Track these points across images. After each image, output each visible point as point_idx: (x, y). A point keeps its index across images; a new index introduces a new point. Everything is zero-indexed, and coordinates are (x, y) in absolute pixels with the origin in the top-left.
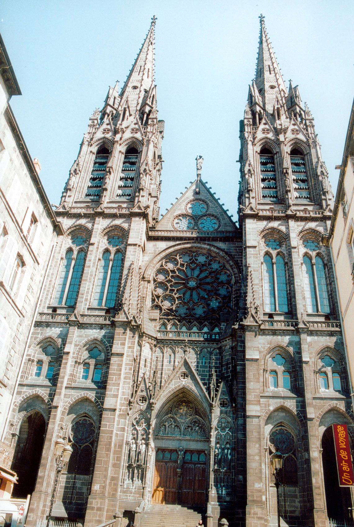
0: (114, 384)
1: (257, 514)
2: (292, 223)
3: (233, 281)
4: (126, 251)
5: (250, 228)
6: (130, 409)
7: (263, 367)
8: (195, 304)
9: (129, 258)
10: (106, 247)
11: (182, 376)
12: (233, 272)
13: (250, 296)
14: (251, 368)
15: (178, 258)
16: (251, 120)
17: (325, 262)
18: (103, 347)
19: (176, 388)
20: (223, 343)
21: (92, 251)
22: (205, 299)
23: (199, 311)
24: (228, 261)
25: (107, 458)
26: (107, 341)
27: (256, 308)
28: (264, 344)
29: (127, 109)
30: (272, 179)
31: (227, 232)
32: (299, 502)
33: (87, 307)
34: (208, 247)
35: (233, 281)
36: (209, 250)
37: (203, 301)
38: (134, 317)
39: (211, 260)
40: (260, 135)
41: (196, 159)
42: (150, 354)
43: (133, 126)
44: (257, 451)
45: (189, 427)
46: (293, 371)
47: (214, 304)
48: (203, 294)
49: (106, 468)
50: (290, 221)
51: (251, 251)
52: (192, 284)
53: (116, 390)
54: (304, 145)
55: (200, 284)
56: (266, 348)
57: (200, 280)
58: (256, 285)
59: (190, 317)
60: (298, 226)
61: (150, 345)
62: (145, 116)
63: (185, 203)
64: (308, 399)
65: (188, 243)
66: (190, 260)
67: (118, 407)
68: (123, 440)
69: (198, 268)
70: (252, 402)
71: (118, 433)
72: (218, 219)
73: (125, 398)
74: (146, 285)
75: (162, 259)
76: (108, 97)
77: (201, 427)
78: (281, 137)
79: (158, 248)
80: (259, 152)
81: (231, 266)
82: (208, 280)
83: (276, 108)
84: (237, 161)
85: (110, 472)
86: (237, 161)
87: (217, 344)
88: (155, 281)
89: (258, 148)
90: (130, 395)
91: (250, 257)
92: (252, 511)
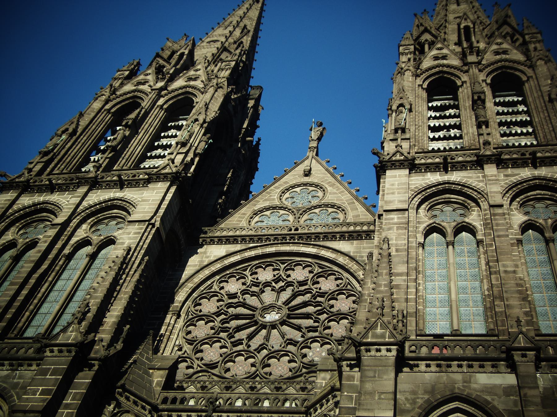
2: (491, 170)
9: (123, 243)
10: (85, 235)
15: (247, 273)
28: (414, 392)
37: (290, 348)
50: (485, 166)
51: (393, 219)
52: (272, 317)
54: (522, 67)
55: (289, 317)
56: (420, 401)
57: (291, 309)
58: (400, 274)
63: (278, 191)
72: (343, 210)
79: (207, 257)
91: (389, 229)
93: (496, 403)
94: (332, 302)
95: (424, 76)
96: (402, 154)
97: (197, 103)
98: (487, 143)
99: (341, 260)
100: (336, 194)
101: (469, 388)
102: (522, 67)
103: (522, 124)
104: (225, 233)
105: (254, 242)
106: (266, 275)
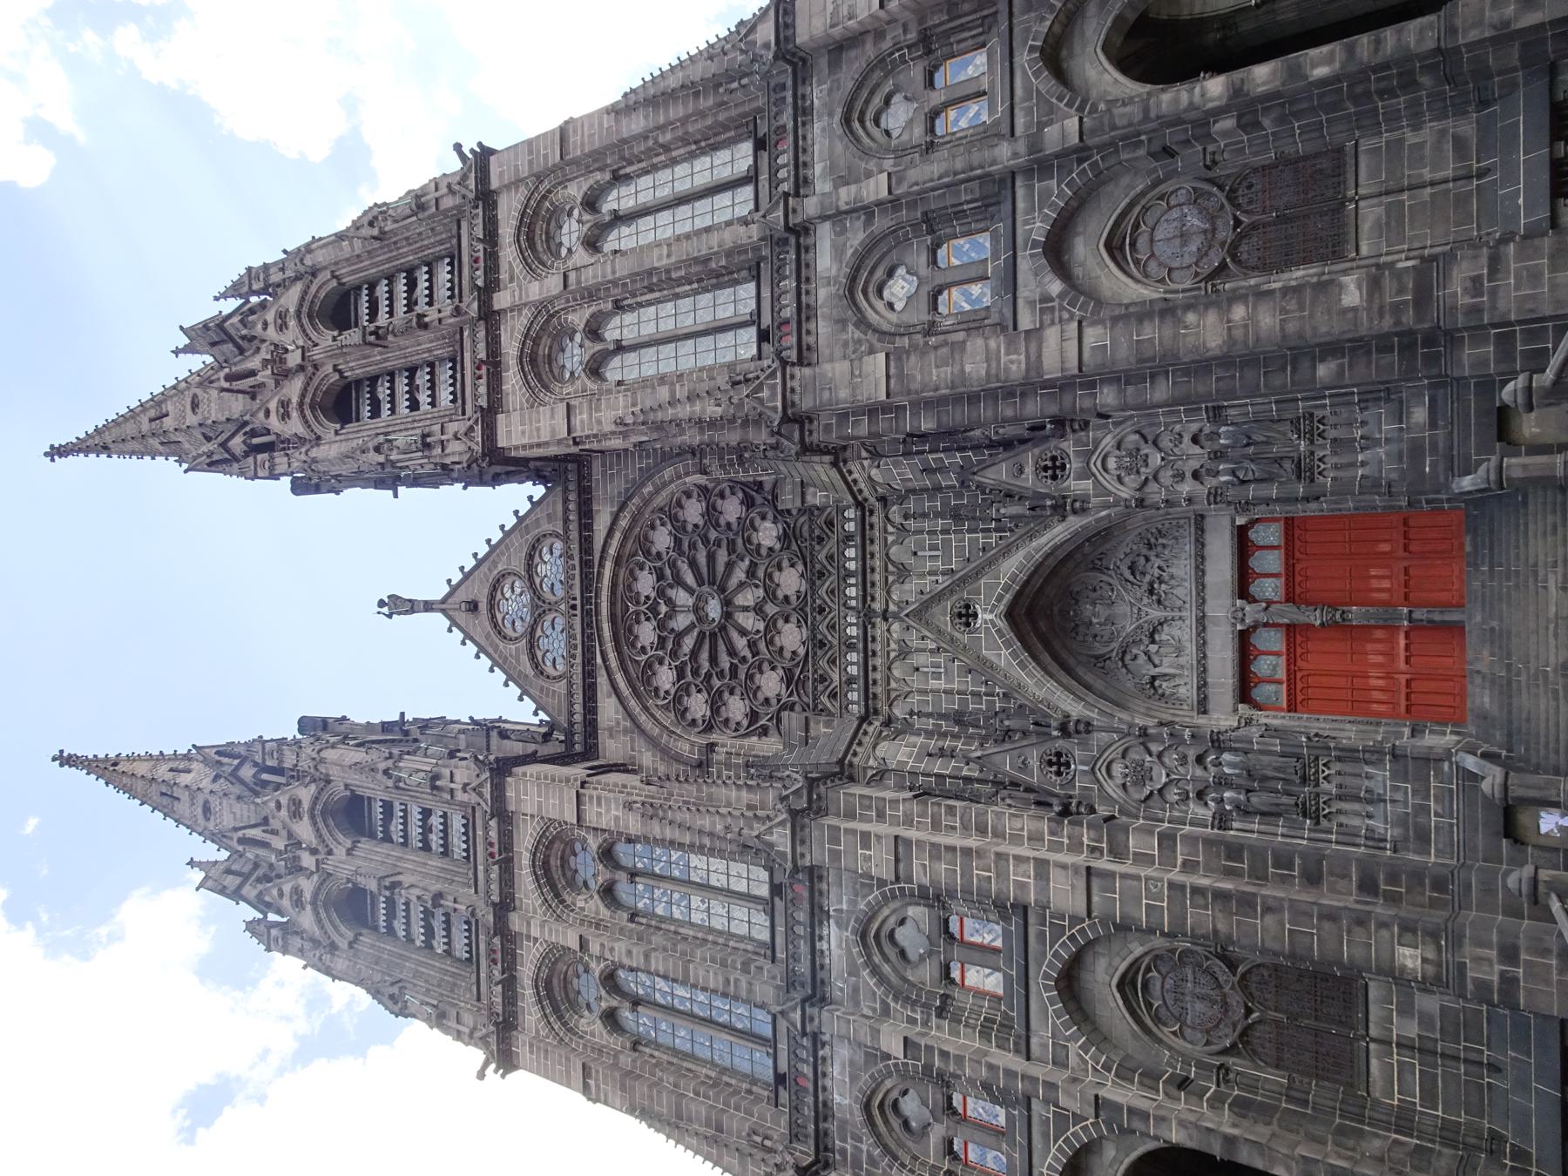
0: (1002, 875)
1: (1476, 280)
2: (501, 300)
3: (700, 479)
4: (604, 831)
5: (523, 433)
6: (1092, 810)
7: (919, 338)
8: (771, 594)
9: (617, 818)
10: (596, 897)
11: (968, 624)
12: (672, 481)
13: (703, 410)
14: (919, 377)
15: (644, 657)
16: (260, 457)
17: (608, 176)
18: (886, 912)
19: (1008, 644)
20: (866, 493)
21: (602, 945)
22: (753, 565)
23: (790, 581)
24: (647, 502)
25: (1280, 910)
26: (865, 897)
27: (735, 384)
28: (846, 344)
29: (240, 834)
30: (411, 378)
31: (566, 510)
32: (1416, 127)
33: (767, 965)
34: (609, 565)
35: (700, 479)
36: (617, 562)
37: (761, 573)
38: (783, 799)
39: (647, 553)
40: (295, 426)
41: (390, 616)
42: (913, 739)
43: (284, 813)
44: (1212, 317)
45: (1151, 591)
46: (931, 231)
47: (768, 534)
48: (739, 574)
49: (1321, 917)
50: (496, 308)
51: (582, 421)
52: (714, 609)
53: (1023, 867)
54: (313, 289)
56: (858, 334)
57: (700, 583)
58: (673, 393)
59: (808, 609)
60: (512, 279)
61: (885, 739)
62: (265, 776)
63: (501, 645)
64: (1016, 155)
65: (599, 629)
66: (648, 619)
67: (1081, 859)
68: (1208, 842)
69: (671, 593)
70: (1033, 358)
71: (1179, 862)
73: (1052, 833)
74: (722, 757)
75: (646, 708)
76: (222, 891)
77: (1150, 546)
78: (294, 359)
79: (618, 723)
80: (338, 426)
81: (657, 491)
82: (702, 559)
83: (226, 385)
84: (396, 496)
85: (1344, 898)
86: (396, 496)
87: (871, 512)
88: (709, 728)
89: (328, 429)
90: (1041, 811)
91: (599, 422)
92: (1464, 300)
93: (856, 243)
94: (690, 528)
95: (319, 430)
96: (471, 429)
97: (346, 786)
98: (457, 311)
99: (624, 523)
100: (509, 557)
101: (836, 278)
102: (313, 289)
103: (412, 285)
104: (578, 708)
105: (594, 658)
106: (647, 633)
